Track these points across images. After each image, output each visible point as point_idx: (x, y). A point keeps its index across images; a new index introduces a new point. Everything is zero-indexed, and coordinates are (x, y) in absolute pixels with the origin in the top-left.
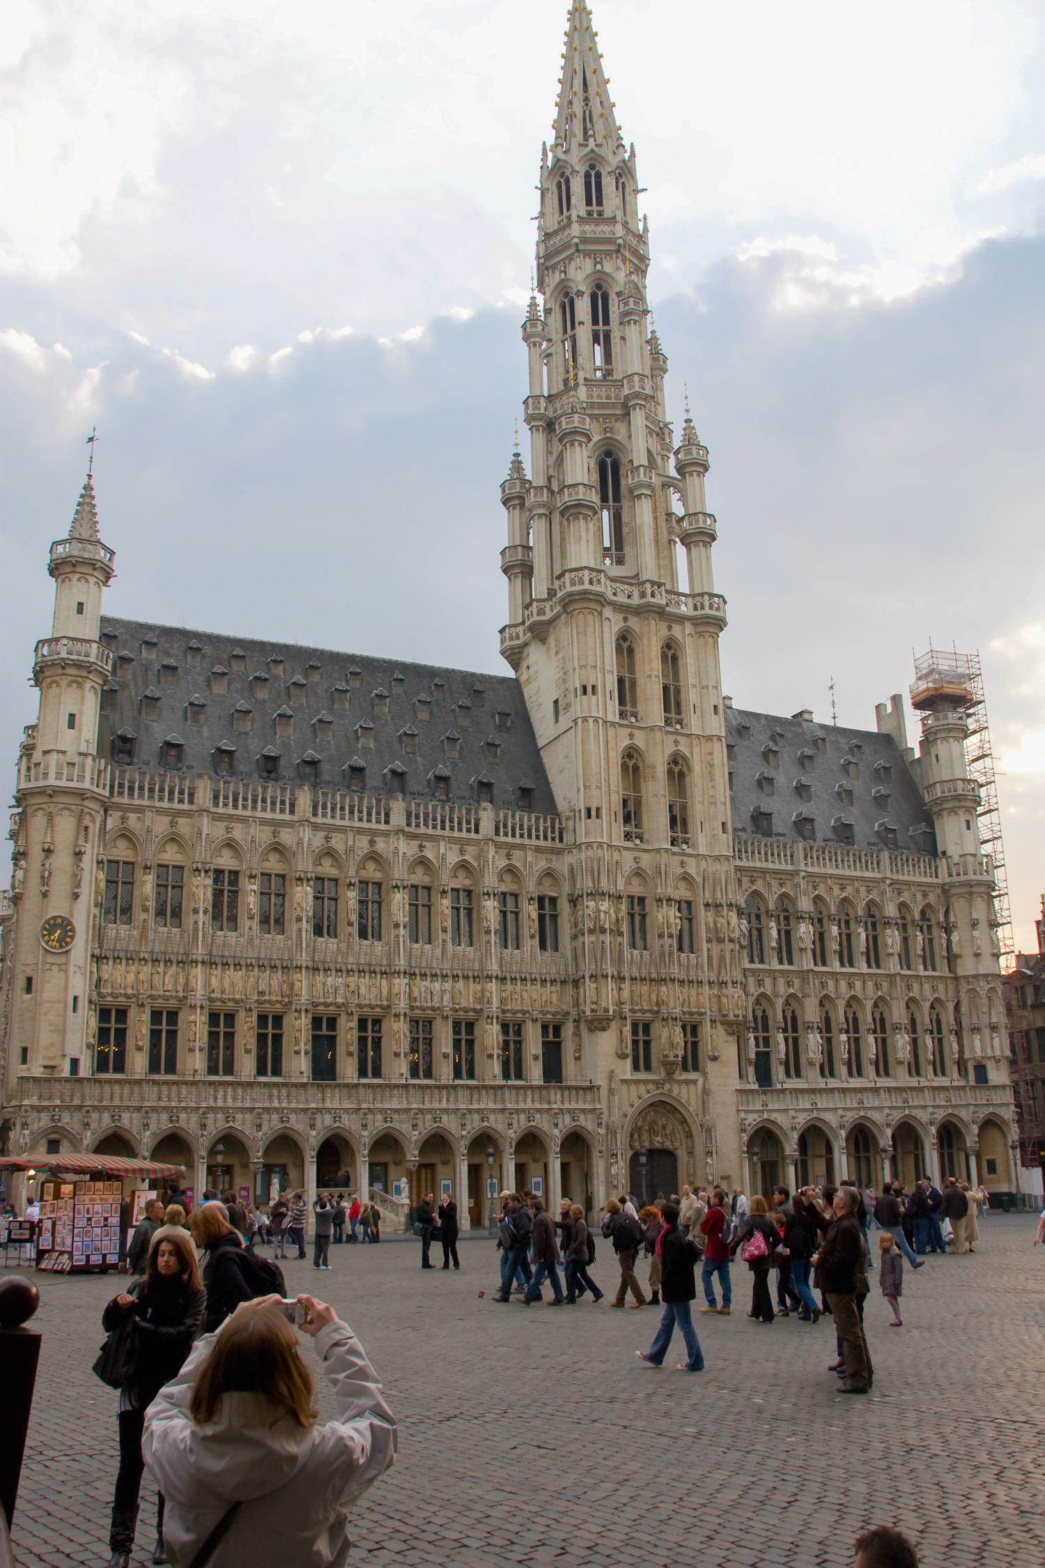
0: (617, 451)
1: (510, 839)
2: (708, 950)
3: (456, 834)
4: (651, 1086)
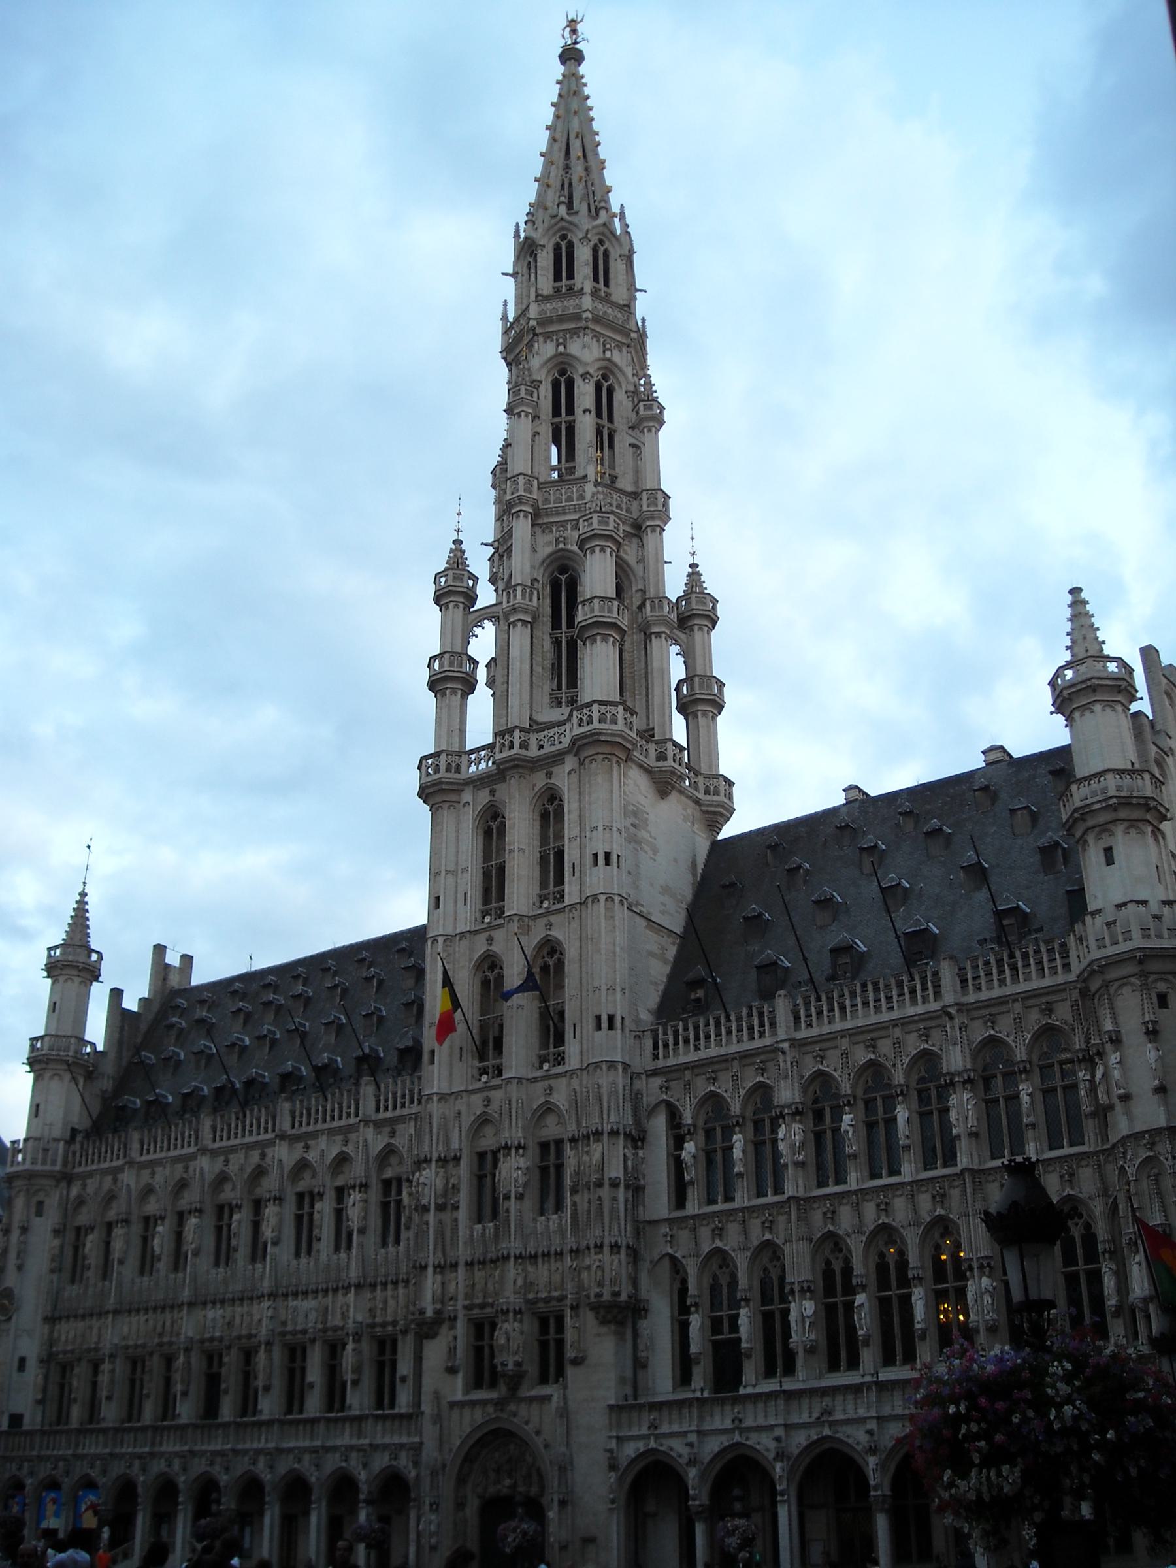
0: (571, 563)
1: (389, 1114)
2: (574, 1204)
3: (336, 1124)
4: (490, 1409)
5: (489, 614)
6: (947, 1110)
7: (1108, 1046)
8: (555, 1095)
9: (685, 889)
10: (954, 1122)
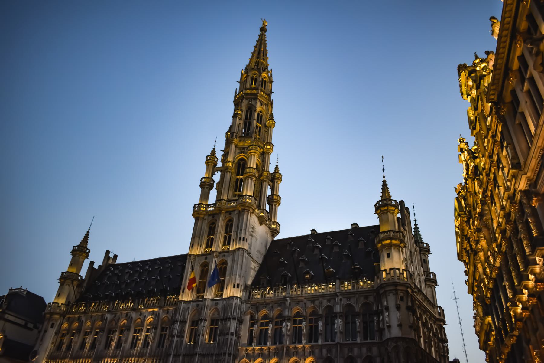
2: (219, 340)
5: (219, 169)
6: (334, 324)
7: (384, 311)
8: (218, 306)
9: (264, 252)
10: (336, 328)
